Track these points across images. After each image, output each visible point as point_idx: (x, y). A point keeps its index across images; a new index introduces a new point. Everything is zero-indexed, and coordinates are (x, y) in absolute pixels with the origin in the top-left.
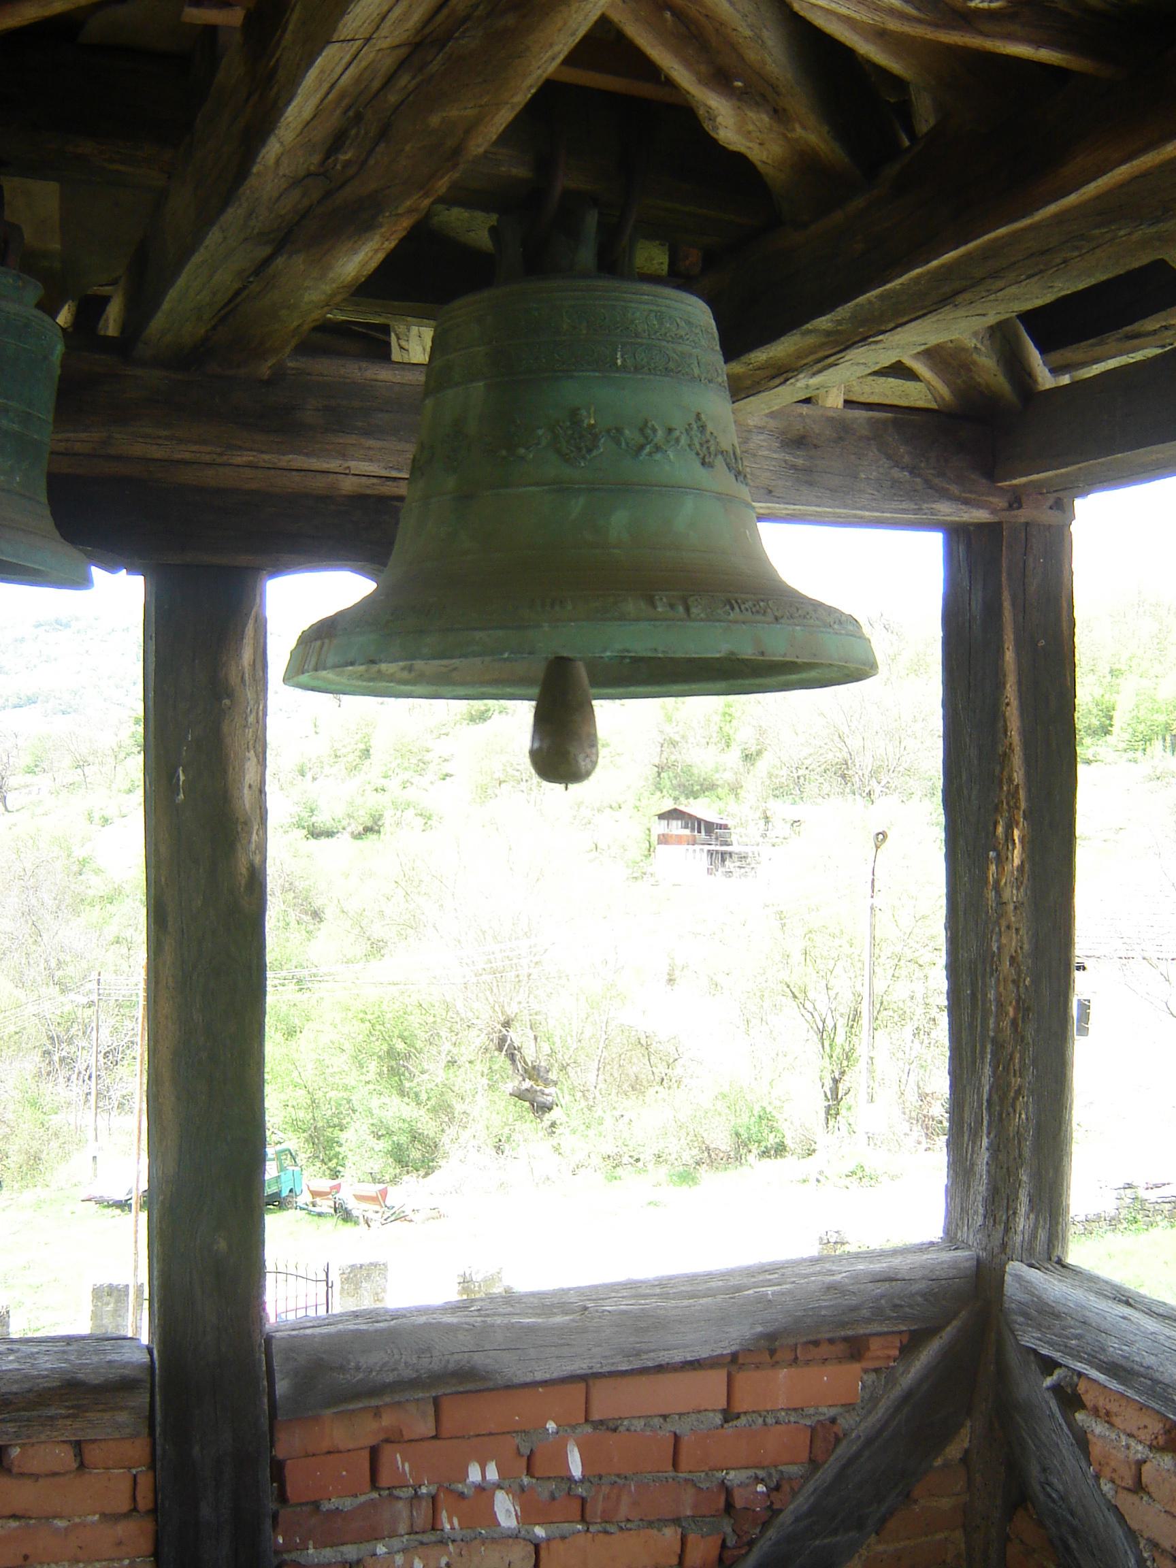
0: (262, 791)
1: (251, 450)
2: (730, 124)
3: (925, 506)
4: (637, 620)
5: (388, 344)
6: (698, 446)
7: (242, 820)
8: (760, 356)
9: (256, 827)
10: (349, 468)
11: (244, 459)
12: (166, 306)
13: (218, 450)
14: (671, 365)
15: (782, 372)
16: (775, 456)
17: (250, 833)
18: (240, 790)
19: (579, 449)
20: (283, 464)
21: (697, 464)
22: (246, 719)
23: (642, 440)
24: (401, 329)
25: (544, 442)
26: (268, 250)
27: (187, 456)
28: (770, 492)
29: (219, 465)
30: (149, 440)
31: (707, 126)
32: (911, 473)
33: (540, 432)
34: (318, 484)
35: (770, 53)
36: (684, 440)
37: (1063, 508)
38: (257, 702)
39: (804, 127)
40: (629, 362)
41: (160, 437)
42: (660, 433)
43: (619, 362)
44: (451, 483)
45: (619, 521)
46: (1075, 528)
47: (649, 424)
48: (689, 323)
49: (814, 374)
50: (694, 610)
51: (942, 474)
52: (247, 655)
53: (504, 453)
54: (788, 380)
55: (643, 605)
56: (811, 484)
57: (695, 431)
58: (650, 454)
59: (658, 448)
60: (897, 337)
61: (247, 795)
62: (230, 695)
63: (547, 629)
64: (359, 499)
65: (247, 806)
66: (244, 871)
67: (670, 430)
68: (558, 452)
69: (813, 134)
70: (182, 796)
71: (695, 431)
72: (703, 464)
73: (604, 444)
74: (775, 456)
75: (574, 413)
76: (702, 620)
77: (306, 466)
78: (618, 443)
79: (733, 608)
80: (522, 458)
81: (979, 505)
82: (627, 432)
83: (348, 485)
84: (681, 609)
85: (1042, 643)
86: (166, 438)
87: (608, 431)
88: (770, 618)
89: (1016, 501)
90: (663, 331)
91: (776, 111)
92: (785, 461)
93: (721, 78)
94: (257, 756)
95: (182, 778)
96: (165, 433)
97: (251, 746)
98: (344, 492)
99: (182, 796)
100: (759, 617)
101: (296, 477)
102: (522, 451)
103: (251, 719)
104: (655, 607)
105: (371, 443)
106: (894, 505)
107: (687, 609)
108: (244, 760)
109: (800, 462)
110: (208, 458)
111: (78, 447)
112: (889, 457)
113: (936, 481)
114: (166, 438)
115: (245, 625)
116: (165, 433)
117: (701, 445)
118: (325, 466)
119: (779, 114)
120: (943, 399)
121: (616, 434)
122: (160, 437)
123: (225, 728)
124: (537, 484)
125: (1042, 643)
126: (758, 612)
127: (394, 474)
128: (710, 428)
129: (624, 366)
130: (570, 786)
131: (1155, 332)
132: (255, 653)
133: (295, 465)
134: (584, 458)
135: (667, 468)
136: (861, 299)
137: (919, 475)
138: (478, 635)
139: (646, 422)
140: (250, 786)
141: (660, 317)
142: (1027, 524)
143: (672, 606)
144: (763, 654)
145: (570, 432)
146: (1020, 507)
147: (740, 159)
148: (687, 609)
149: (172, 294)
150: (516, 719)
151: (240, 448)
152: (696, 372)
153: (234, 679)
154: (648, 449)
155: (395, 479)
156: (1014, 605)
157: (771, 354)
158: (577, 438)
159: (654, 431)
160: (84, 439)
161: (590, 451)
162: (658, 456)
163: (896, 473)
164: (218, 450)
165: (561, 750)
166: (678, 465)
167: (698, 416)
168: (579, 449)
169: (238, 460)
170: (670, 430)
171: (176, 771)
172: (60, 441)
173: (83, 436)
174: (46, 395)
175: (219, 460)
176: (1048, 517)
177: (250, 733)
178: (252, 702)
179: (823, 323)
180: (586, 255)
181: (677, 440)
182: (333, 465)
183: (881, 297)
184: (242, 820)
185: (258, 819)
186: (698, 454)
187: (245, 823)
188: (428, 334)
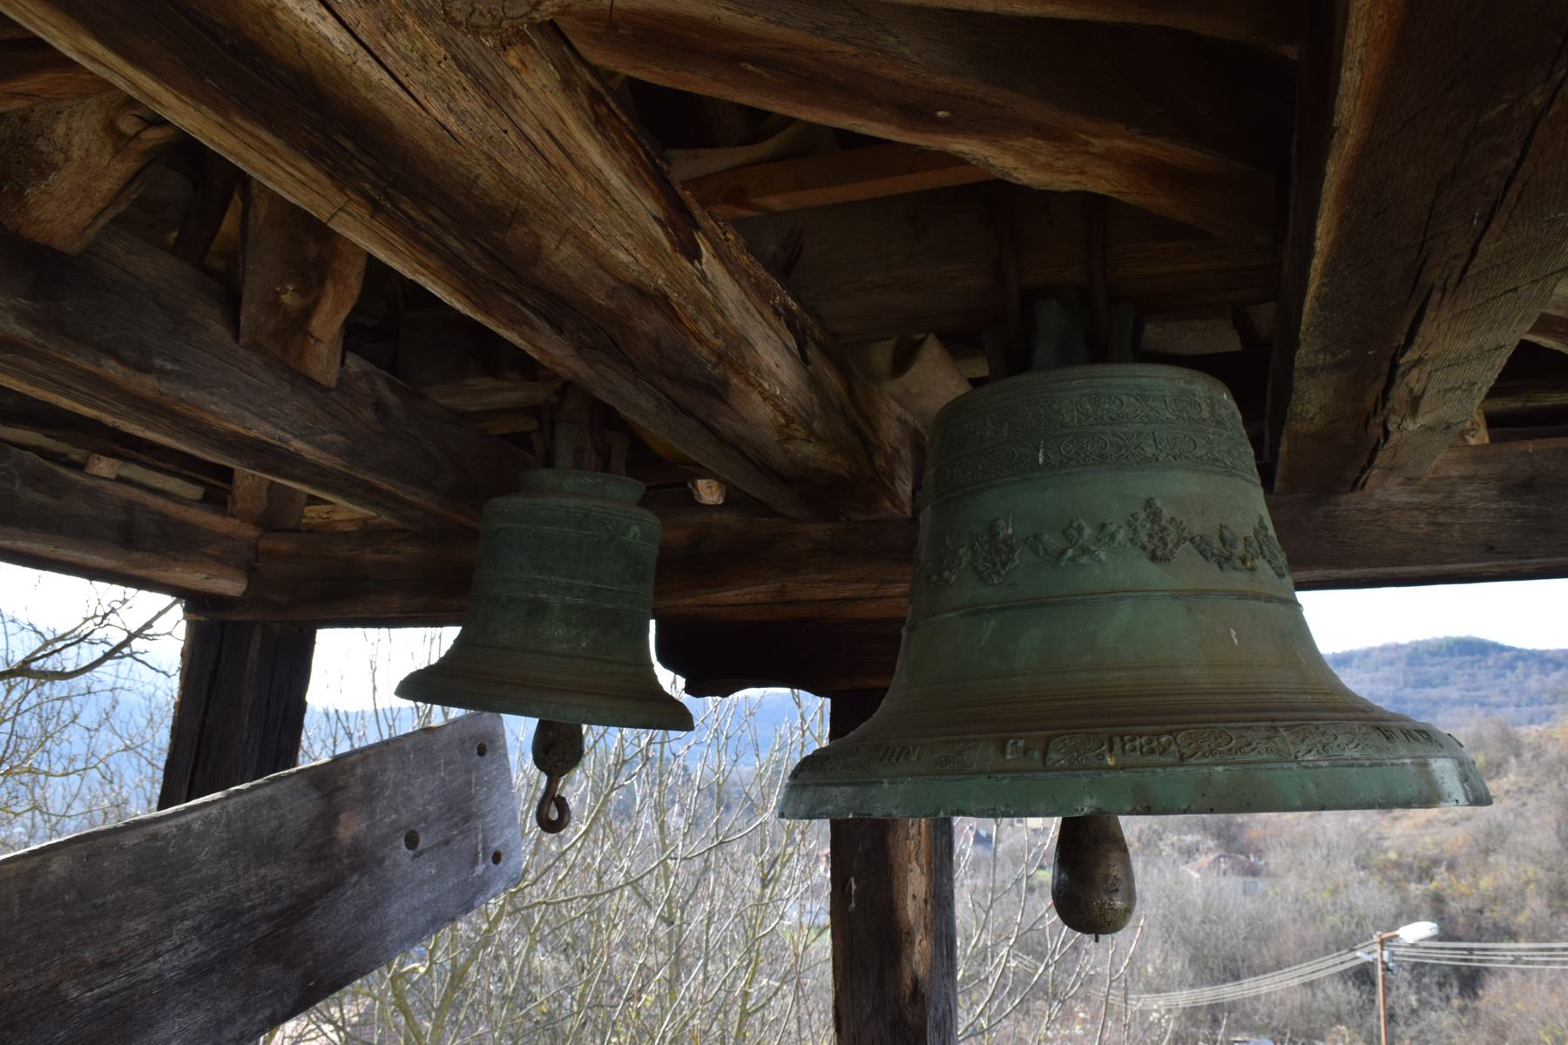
6: (1145, 539)
9: (918, 938)
16: (1494, 506)
17: (912, 943)
25: (965, 562)
27: (847, 594)
28: (1491, 548)
33: (961, 551)
42: (1088, 531)
50: (1053, 756)
53: (934, 578)
58: (1073, 559)
59: (1084, 550)
63: (886, 786)
66: (909, 982)
68: (976, 569)
72: (1153, 558)
74: (1494, 506)
75: (992, 527)
78: (1036, 552)
79: (1111, 750)
82: (1046, 537)
86: (829, 581)
92: (1510, 510)
100: (1156, 758)
104: (1004, 753)
108: (906, 871)
111: (760, 597)
114: (829, 581)
123: (890, 841)
126: (1152, 751)
128: (1166, 513)
130: (1101, 937)
134: (998, 573)
138: (835, 791)
139: (1070, 525)
140: (914, 897)
152: (1150, 451)
154: (1070, 553)
159: (1080, 530)
161: (1004, 565)
162: (1084, 560)
167: (1149, 503)
168: (994, 565)
170: (1103, 526)
173: (763, 588)
181: (1113, 536)
186: (1144, 548)
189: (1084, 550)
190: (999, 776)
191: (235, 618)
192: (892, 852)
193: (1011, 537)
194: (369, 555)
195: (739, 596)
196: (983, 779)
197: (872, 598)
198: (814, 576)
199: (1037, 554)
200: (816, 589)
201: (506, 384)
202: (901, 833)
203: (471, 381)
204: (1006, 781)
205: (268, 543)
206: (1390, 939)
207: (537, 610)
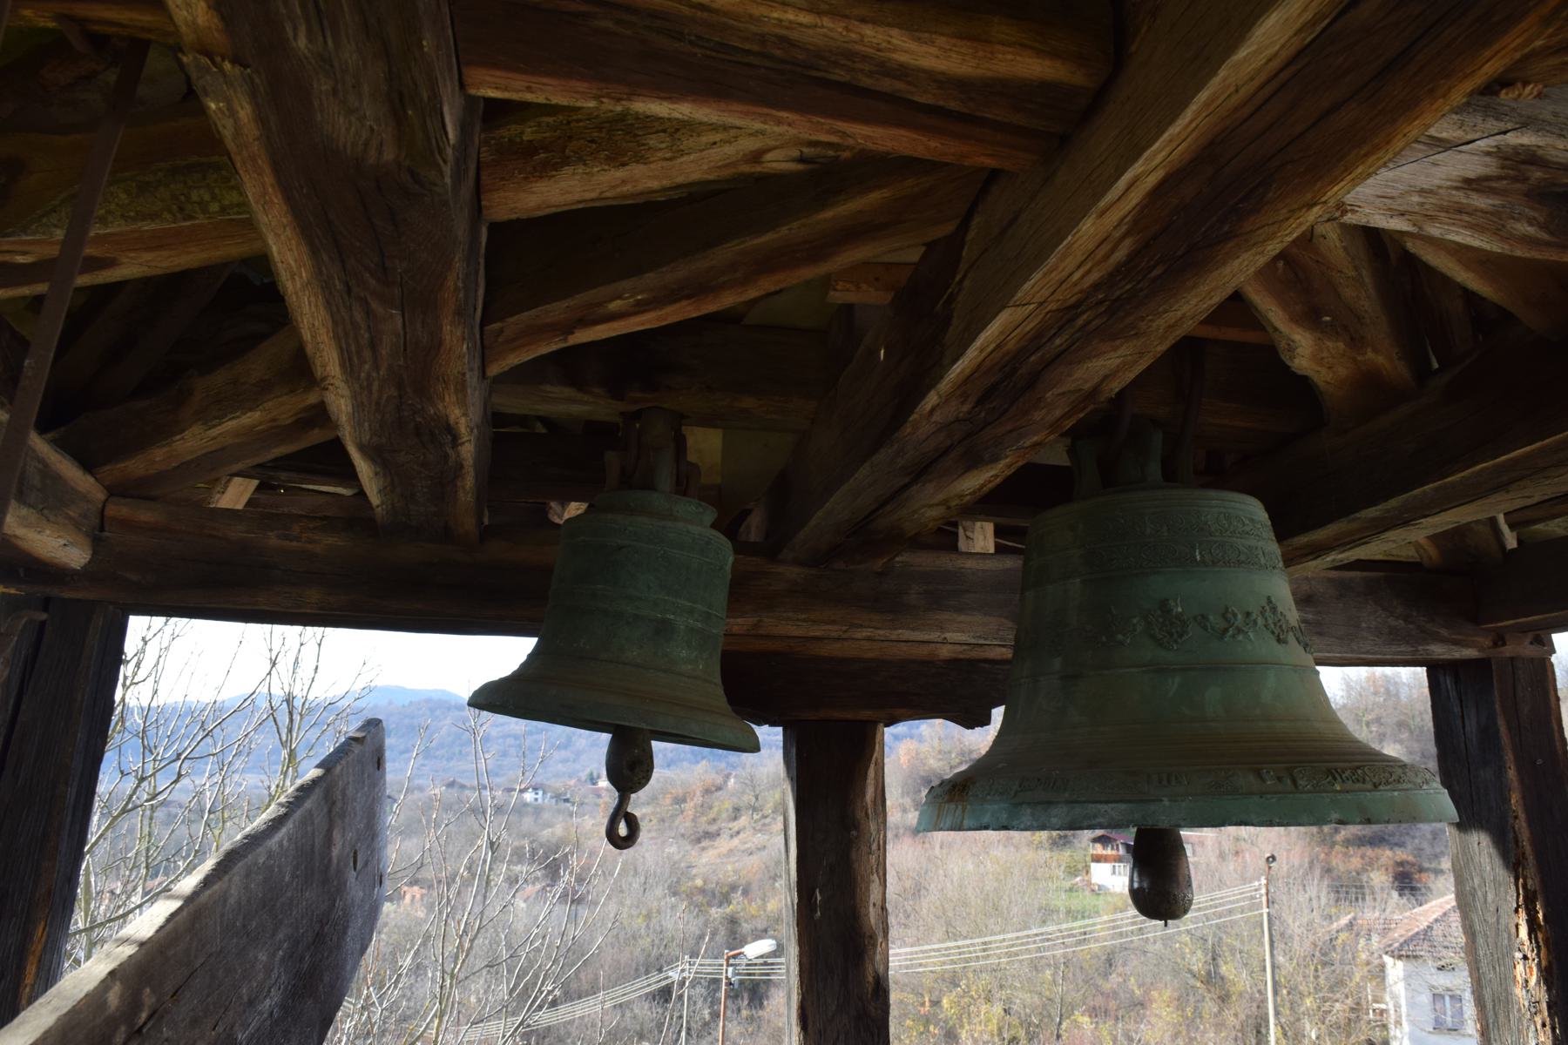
0: (884, 908)
2: (1305, 351)
4: (1252, 794)
5: (956, 534)
8: (1303, 539)
12: (813, 523)
14: (1242, 558)
15: (1317, 551)
17: (875, 946)
18: (867, 908)
19: (1171, 635)
20: (893, 637)
21: (1275, 643)
24: (968, 524)
25: (1139, 629)
26: (907, 480)
31: (1285, 358)
34: (922, 652)
35: (1359, 290)
36: (1260, 621)
38: (878, 831)
39: (1375, 351)
44: (1057, 663)
46: (1554, 659)
48: (1252, 520)
50: (1301, 782)
56: (1320, 634)
57: (1268, 614)
58: (1233, 636)
59: (1239, 631)
61: (873, 914)
63: (1166, 802)
64: (954, 662)
65: (873, 921)
67: (1248, 614)
69: (1384, 358)
72: (1279, 640)
75: (1164, 605)
81: (1467, 646)
83: (945, 652)
85: (1539, 762)
88: (1369, 786)
89: (1500, 640)
91: (1352, 339)
93: (1311, 317)
101: (903, 646)
102: (1120, 637)
103: (874, 847)
104: (1264, 781)
105: (962, 618)
106: (1394, 648)
107: (1294, 782)
108: (869, 883)
109: (1310, 616)
110: (834, 634)
111: (736, 629)
118: (927, 638)
119: (1356, 341)
121: (1202, 620)
123: (854, 856)
125: (1539, 762)
127: (982, 642)
128: (1280, 609)
129: (1203, 561)
133: (904, 638)
136: (1416, 492)
138: (1103, 807)
142: (1512, 659)
143: (1280, 779)
146: (1504, 644)
147: (1303, 382)
148: (1294, 782)
149: (820, 513)
152: (1263, 561)
153: (860, 815)
156: (1510, 729)
159: (1235, 615)
160: (740, 624)
161: (1181, 636)
162: (1240, 637)
163: (1392, 622)
165: (1160, 889)
166: (1260, 645)
168: (1171, 635)
169: (858, 636)
173: (739, 620)
174: (721, 596)
176: (1528, 650)
177: (873, 859)
179: (1372, 512)
180: (1154, 469)
181: (1255, 622)
183: (1436, 489)
188: (989, 528)
189: (1239, 631)
191: (67, 595)
192: (856, 865)
194: (273, 540)
196: (1256, 798)
201: (586, 398)
202: (864, 849)
203: (548, 388)
205: (120, 510)
206: (734, 957)
207: (663, 630)
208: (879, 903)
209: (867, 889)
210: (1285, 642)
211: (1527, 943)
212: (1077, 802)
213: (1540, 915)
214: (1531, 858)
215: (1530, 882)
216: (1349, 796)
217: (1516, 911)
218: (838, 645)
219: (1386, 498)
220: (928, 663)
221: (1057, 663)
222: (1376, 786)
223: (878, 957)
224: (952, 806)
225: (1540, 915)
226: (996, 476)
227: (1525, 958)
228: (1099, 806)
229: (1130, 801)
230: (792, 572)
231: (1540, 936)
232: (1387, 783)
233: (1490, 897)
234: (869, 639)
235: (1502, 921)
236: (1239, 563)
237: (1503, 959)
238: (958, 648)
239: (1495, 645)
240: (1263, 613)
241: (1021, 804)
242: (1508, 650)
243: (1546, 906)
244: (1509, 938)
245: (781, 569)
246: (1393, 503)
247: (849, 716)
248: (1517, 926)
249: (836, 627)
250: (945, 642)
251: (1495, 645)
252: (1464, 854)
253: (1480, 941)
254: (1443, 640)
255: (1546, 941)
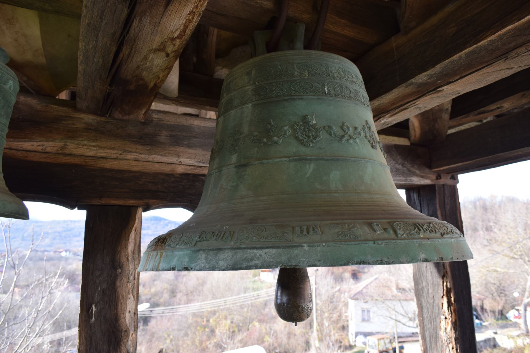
1: (135, 152)
3: (408, 178)
4: (367, 240)
7: (124, 329)
9: (131, 333)
10: (180, 162)
11: (132, 157)
13: (120, 152)
14: (352, 95)
17: (128, 336)
18: (124, 314)
19: (309, 137)
20: (150, 159)
21: (371, 147)
22: (129, 279)
23: (342, 133)
29: (120, 159)
30: (85, 147)
32: (402, 166)
33: (286, 128)
34: (167, 169)
36: (362, 134)
37: (455, 179)
40: (332, 92)
41: (90, 146)
43: (326, 91)
44: (234, 158)
45: (335, 177)
46: (458, 186)
47: (345, 124)
49: (392, 116)
50: (400, 232)
51: (413, 166)
52: (131, 247)
53: (265, 140)
54: (379, 119)
55: (366, 229)
57: (366, 130)
58: (347, 140)
59: (351, 137)
60: (453, 87)
62: (121, 267)
63: (306, 248)
64: (185, 176)
67: (356, 128)
68: (297, 138)
70: (94, 319)
71: (366, 130)
72: (372, 147)
73: (323, 135)
75: (305, 120)
76: (405, 239)
77: (161, 160)
79: (420, 230)
80: (276, 143)
81: (427, 178)
82: (334, 128)
83: (180, 170)
84: (392, 232)
87: (324, 128)
88: (438, 235)
89: (439, 177)
90: (346, 78)
94: (134, 296)
95: (94, 309)
96: (94, 144)
97: (131, 292)
98: (178, 172)
99: (94, 319)
100: (433, 235)
101: (157, 166)
102: (275, 138)
103: (131, 278)
104: (375, 231)
105: (191, 151)
107: (395, 232)
110: (114, 156)
111: (49, 149)
112: (394, 160)
113: (412, 169)
114: (94, 146)
115: (130, 232)
116: (94, 144)
117: (370, 137)
120: (415, 136)
121: (328, 129)
122: (90, 146)
123: (118, 283)
124: (285, 157)
127: (201, 165)
129: (329, 94)
130: (298, 323)
131: (492, 110)
132: (135, 245)
134: (312, 141)
135: (357, 148)
136: (455, 57)
137: (405, 167)
139: (343, 124)
140: (129, 312)
141: (344, 71)
142: (443, 185)
143: (385, 230)
144: (442, 259)
145: (303, 128)
146: (440, 178)
148: (395, 232)
150: (294, 324)
151: (130, 152)
152: (363, 101)
153: (123, 260)
154: (346, 138)
155: (201, 167)
157: (382, 102)
158: (306, 131)
159: (348, 128)
161: (315, 138)
162: (351, 141)
163: (397, 166)
164: (120, 152)
168: (309, 137)
171: (91, 306)
172: (40, 146)
173: (51, 144)
175: (120, 157)
176: (449, 182)
177: (130, 285)
178: (132, 270)
179: (422, 78)
181: (360, 134)
182: (174, 160)
183: (468, 55)
184: (124, 329)
185: (133, 329)
186: (369, 141)
187: (126, 331)
189: (351, 137)
190: (380, 242)
192: (119, 289)
193: (316, 124)
195: (37, 147)
196: (371, 244)
197: (116, 159)
198: (86, 142)
199: (331, 135)
200: (85, 150)
202: (125, 279)
204: (383, 245)
208: (133, 311)
209: (126, 303)
210: (376, 148)
211: (447, 311)
212: (240, 248)
213: (453, 299)
214: (449, 273)
215: (448, 284)
216: (429, 242)
217: (443, 297)
218: (116, 162)
219: (434, 66)
220: (170, 175)
221: (234, 158)
222: (442, 235)
223: (130, 343)
224: (155, 253)
225: (453, 299)
226: (192, 13)
227: (446, 318)
228: (256, 251)
229: (279, 247)
230: (89, 118)
231: (452, 308)
232: (447, 233)
233: (430, 291)
234: (135, 160)
235: (436, 302)
236: (351, 98)
237: (435, 319)
238: (187, 167)
239: (437, 179)
240: (364, 129)
241: (198, 251)
242: (442, 181)
243: (455, 295)
244: (439, 309)
245: (82, 116)
246: (438, 68)
247: (121, 202)
248: (442, 304)
249: (115, 152)
250: (180, 164)
251: (437, 179)
252: (419, 272)
253: (425, 310)
254: (417, 176)
255: (454, 310)
